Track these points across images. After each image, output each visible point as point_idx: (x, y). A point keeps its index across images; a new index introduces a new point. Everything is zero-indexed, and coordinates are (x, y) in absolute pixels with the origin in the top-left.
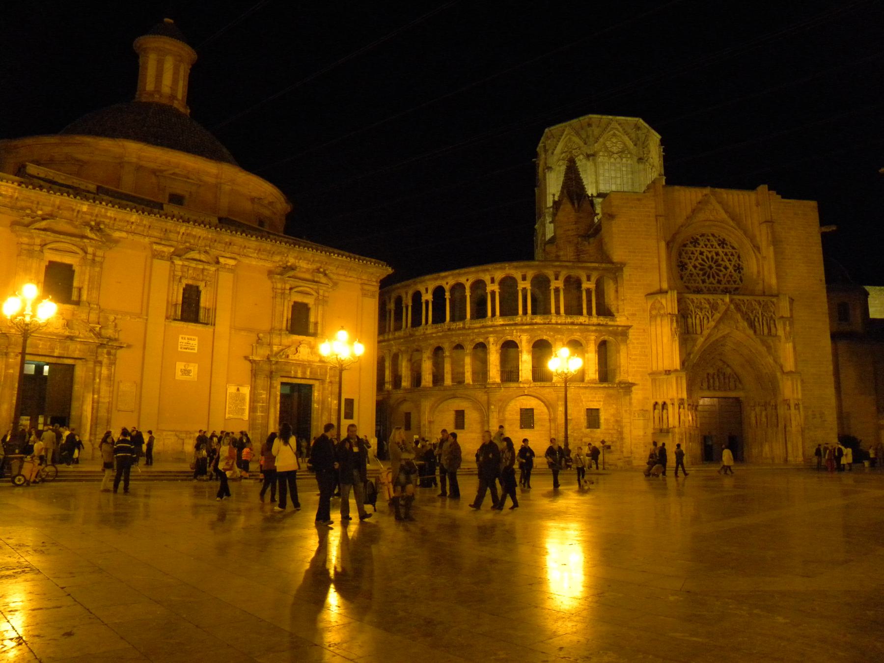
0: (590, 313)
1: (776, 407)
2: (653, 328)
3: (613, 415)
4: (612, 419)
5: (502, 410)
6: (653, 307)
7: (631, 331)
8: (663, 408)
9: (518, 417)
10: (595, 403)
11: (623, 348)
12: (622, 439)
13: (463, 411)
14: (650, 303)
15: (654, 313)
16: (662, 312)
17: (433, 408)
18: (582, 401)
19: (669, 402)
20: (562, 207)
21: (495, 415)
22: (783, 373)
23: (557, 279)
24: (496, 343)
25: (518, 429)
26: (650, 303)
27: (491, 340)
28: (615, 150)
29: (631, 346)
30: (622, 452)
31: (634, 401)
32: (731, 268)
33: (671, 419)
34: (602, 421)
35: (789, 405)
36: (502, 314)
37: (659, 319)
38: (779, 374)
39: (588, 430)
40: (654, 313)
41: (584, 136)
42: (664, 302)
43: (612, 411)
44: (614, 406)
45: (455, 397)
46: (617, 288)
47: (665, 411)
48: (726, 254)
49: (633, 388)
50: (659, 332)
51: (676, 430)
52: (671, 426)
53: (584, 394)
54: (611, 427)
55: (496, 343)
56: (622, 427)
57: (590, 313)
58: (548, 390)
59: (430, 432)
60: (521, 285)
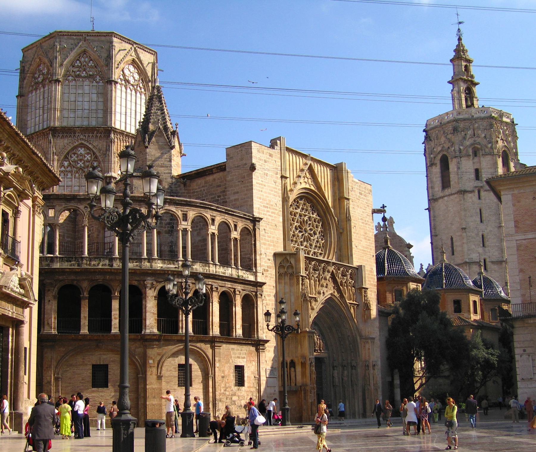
0: (236, 264)
1: (353, 367)
3: (253, 373)
5: (159, 364)
7: (264, 287)
8: (290, 367)
9: (176, 374)
10: (241, 360)
11: (259, 303)
14: (279, 260)
15: (282, 271)
16: (290, 271)
18: (231, 357)
19: (296, 360)
21: (154, 370)
22: (361, 336)
23: (213, 224)
27: (149, 282)
29: (264, 302)
33: (299, 378)
34: (246, 379)
35: (368, 366)
36: (161, 256)
38: (358, 338)
39: (237, 388)
41: (104, 55)
42: (293, 261)
44: (254, 363)
47: (293, 369)
48: (315, 221)
53: (233, 349)
54: (252, 385)
57: (236, 264)
60: (184, 225)
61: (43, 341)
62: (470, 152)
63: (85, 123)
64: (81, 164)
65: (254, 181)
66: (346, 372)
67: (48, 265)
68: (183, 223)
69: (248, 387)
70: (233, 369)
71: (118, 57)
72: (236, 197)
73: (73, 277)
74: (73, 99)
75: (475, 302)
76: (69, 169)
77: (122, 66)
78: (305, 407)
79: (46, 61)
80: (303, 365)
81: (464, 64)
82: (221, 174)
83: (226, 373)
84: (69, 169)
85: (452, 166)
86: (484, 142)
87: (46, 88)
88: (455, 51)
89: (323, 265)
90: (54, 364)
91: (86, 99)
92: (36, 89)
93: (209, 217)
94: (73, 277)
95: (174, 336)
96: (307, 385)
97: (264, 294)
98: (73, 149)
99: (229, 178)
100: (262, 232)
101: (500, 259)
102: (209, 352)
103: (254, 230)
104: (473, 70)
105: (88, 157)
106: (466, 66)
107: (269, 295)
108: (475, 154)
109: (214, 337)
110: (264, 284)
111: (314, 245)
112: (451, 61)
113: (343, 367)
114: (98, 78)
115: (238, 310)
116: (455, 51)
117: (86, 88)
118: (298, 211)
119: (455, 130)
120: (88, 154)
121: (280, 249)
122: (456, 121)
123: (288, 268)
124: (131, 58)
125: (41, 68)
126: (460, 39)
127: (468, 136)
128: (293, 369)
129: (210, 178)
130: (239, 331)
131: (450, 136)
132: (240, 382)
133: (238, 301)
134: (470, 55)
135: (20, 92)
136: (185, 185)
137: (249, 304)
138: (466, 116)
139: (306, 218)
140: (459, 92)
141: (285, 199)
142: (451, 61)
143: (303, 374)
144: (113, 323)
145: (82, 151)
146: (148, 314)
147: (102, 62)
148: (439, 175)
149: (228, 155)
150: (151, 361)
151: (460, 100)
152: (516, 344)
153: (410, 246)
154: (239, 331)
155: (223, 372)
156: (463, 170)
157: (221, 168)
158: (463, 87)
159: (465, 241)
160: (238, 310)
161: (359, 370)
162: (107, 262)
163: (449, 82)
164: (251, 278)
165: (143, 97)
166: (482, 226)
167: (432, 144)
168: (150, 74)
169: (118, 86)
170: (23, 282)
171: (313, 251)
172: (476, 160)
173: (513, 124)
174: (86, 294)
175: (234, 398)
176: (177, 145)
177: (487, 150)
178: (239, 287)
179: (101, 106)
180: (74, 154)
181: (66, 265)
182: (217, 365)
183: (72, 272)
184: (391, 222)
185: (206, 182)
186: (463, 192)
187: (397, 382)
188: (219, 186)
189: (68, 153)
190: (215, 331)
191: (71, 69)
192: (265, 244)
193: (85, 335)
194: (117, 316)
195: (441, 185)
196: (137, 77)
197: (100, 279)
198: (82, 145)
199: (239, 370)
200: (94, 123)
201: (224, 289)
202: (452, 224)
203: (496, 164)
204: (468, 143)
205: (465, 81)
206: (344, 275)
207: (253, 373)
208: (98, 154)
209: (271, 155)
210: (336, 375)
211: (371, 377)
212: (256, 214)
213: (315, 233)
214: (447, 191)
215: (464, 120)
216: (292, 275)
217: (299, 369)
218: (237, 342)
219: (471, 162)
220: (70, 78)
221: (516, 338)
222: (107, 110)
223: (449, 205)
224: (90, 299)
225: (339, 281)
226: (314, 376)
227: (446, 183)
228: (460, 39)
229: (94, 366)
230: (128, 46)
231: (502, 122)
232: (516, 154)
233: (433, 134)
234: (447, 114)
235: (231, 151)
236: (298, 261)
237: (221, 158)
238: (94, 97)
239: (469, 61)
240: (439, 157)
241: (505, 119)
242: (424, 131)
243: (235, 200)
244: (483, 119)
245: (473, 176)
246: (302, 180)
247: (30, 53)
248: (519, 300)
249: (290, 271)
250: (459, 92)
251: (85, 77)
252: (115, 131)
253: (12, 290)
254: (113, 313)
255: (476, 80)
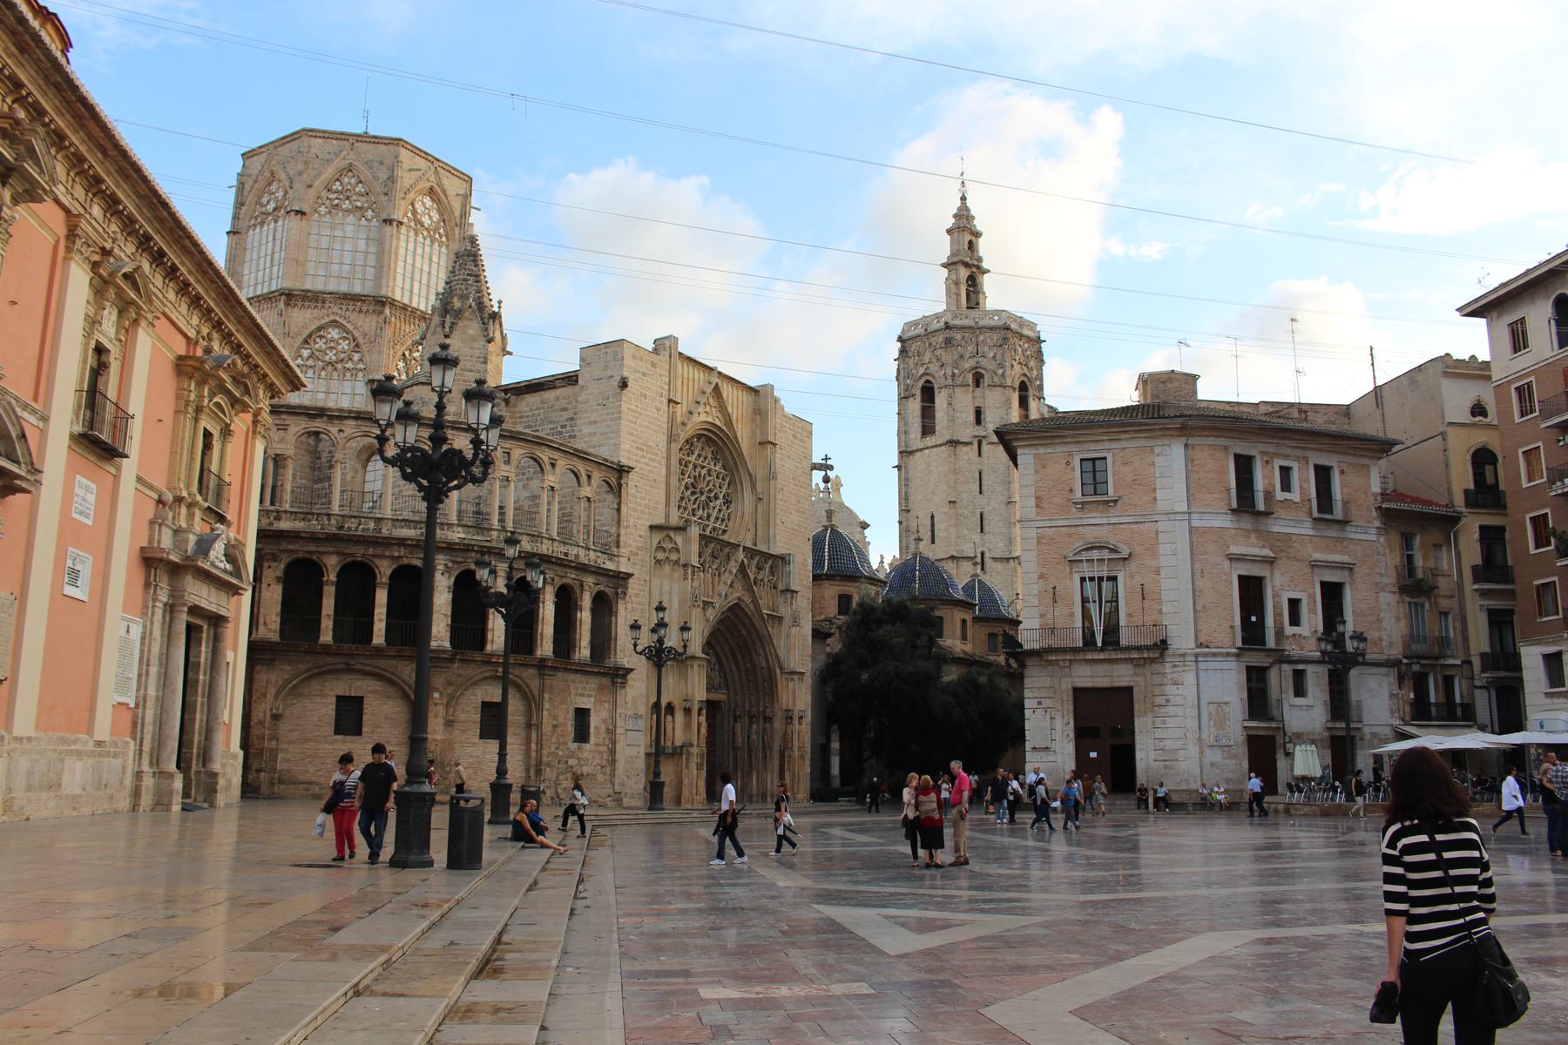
1: (768, 719)
2: (656, 582)
3: (604, 721)
4: (603, 727)
5: (451, 702)
6: (660, 548)
7: (631, 581)
9: (478, 717)
11: (621, 607)
12: (613, 762)
13: (359, 701)
15: (661, 556)
16: (674, 557)
17: (292, 690)
19: (676, 704)
20: (460, 324)
21: (441, 709)
24: (448, 570)
25: (476, 739)
26: (657, 537)
27: (441, 561)
28: (426, 221)
30: (613, 784)
31: (629, 699)
32: (721, 500)
33: (679, 732)
34: (592, 730)
37: (667, 568)
39: (576, 745)
40: (661, 556)
41: (383, 176)
43: (604, 714)
45: (349, 670)
46: (619, 504)
49: (631, 676)
50: (666, 588)
51: (695, 750)
52: (678, 743)
55: (448, 570)
56: (614, 742)
58: (532, 671)
59: (275, 737)
61: (258, 653)
62: (970, 380)
63: (344, 288)
64: (331, 356)
65: (624, 406)
66: (754, 726)
67: (271, 524)
68: (504, 467)
69: (597, 745)
70: (571, 715)
71: (405, 179)
72: (592, 429)
73: (312, 548)
74: (324, 245)
75: (964, 621)
76: (310, 362)
77: (411, 196)
78: (686, 781)
79: (283, 177)
80: (687, 711)
81: (968, 237)
82: (568, 390)
83: (561, 719)
84: (310, 362)
85: (940, 400)
86: (992, 366)
87: (280, 223)
88: (955, 216)
89: (727, 550)
90: (272, 691)
91: (348, 247)
92: (263, 223)
93: (545, 459)
94: (312, 548)
95: (478, 656)
96: (691, 745)
97: (630, 591)
98: (319, 329)
99: (582, 398)
100: (632, 491)
101: (1007, 555)
102: (535, 684)
103: (620, 485)
104: (983, 247)
105: (344, 345)
106: (970, 242)
107: (637, 595)
108: (977, 383)
109: (543, 660)
110: (630, 575)
111: (714, 515)
112: (948, 231)
113: (751, 718)
114: (369, 213)
115: (585, 617)
116: (955, 216)
117: (350, 228)
118: (692, 458)
119: (948, 341)
120: (345, 338)
121: (660, 520)
122: (947, 327)
123: (671, 550)
124: (428, 185)
125: (274, 187)
126: (963, 199)
127: (968, 355)
128: (669, 718)
129: (549, 395)
130: (584, 651)
131: (938, 352)
132: (582, 734)
133: (586, 601)
134: (979, 224)
135: (233, 225)
136: (507, 402)
137: (604, 606)
138: (966, 322)
139: (704, 472)
140: (957, 283)
141: (671, 438)
142: (948, 231)
143: (688, 726)
144: (376, 628)
145: (334, 333)
146: (435, 616)
147: (379, 188)
148: (918, 412)
149: (582, 359)
150: (436, 695)
151: (958, 295)
152: (1027, 693)
153: (865, 526)
154: (584, 651)
155: (556, 717)
156: (954, 409)
157: (570, 379)
158: (964, 273)
159: (953, 522)
160: (585, 617)
161: (778, 724)
162: (372, 525)
163: (944, 266)
164: (610, 566)
165: (444, 249)
166: (981, 500)
167: (911, 362)
168: (457, 213)
169: (403, 229)
170: (231, 551)
171: (711, 524)
172: (978, 392)
173: (1039, 341)
174: (333, 577)
175: (572, 762)
176: (498, 335)
177: (996, 379)
178: (589, 580)
179: (372, 261)
180: (321, 337)
181: (299, 525)
182: (547, 706)
183: (313, 538)
184: (838, 485)
185: (542, 402)
186: (954, 443)
187: (835, 745)
188: (565, 410)
189: (310, 336)
190: (545, 648)
191: (324, 194)
192: (635, 510)
193: (326, 646)
194: (384, 617)
195: (920, 429)
196: (436, 217)
197: (358, 552)
198: (334, 324)
199: (582, 715)
200: (357, 289)
201: (565, 581)
202: (934, 494)
203: (1009, 401)
204: (967, 366)
205: (967, 265)
206: (759, 568)
207: (604, 721)
208: (361, 340)
209: (653, 365)
210: (738, 730)
211: (796, 737)
212: (624, 461)
213: (716, 498)
214: (930, 441)
215: (963, 328)
216: (676, 563)
217: (679, 716)
218: (581, 670)
219: (970, 396)
220: (323, 209)
221: (1027, 681)
222: (382, 265)
223: (933, 462)
224: (338, 585)
225: (752, 576)
226: (704, 731)
227: (928, 429)
228: (963, 199)
229: (339, 698)
230: (423, 164)
231: (1021, 336)
232: (1041, 388)
233: (913, 347)
234: (937, 316)
235: (590, 353)
236: (687, 541)
237: (571, 364)
238: (362, 245)
239: (978, 235)
240: (921, 383)
241: (1026, 332)
242: (900, 339)
243: (591, 434)
244: (991, 329)
245: (972, 418)
246: (701, 410)
247: (256, 164)
248: (1035, 623)
249: (674, 557)
250: (957, 283)
251: (347, 211)
252: (392, 303)
253: (213, 564)
254: (377, 611)
255: (985, 265)
